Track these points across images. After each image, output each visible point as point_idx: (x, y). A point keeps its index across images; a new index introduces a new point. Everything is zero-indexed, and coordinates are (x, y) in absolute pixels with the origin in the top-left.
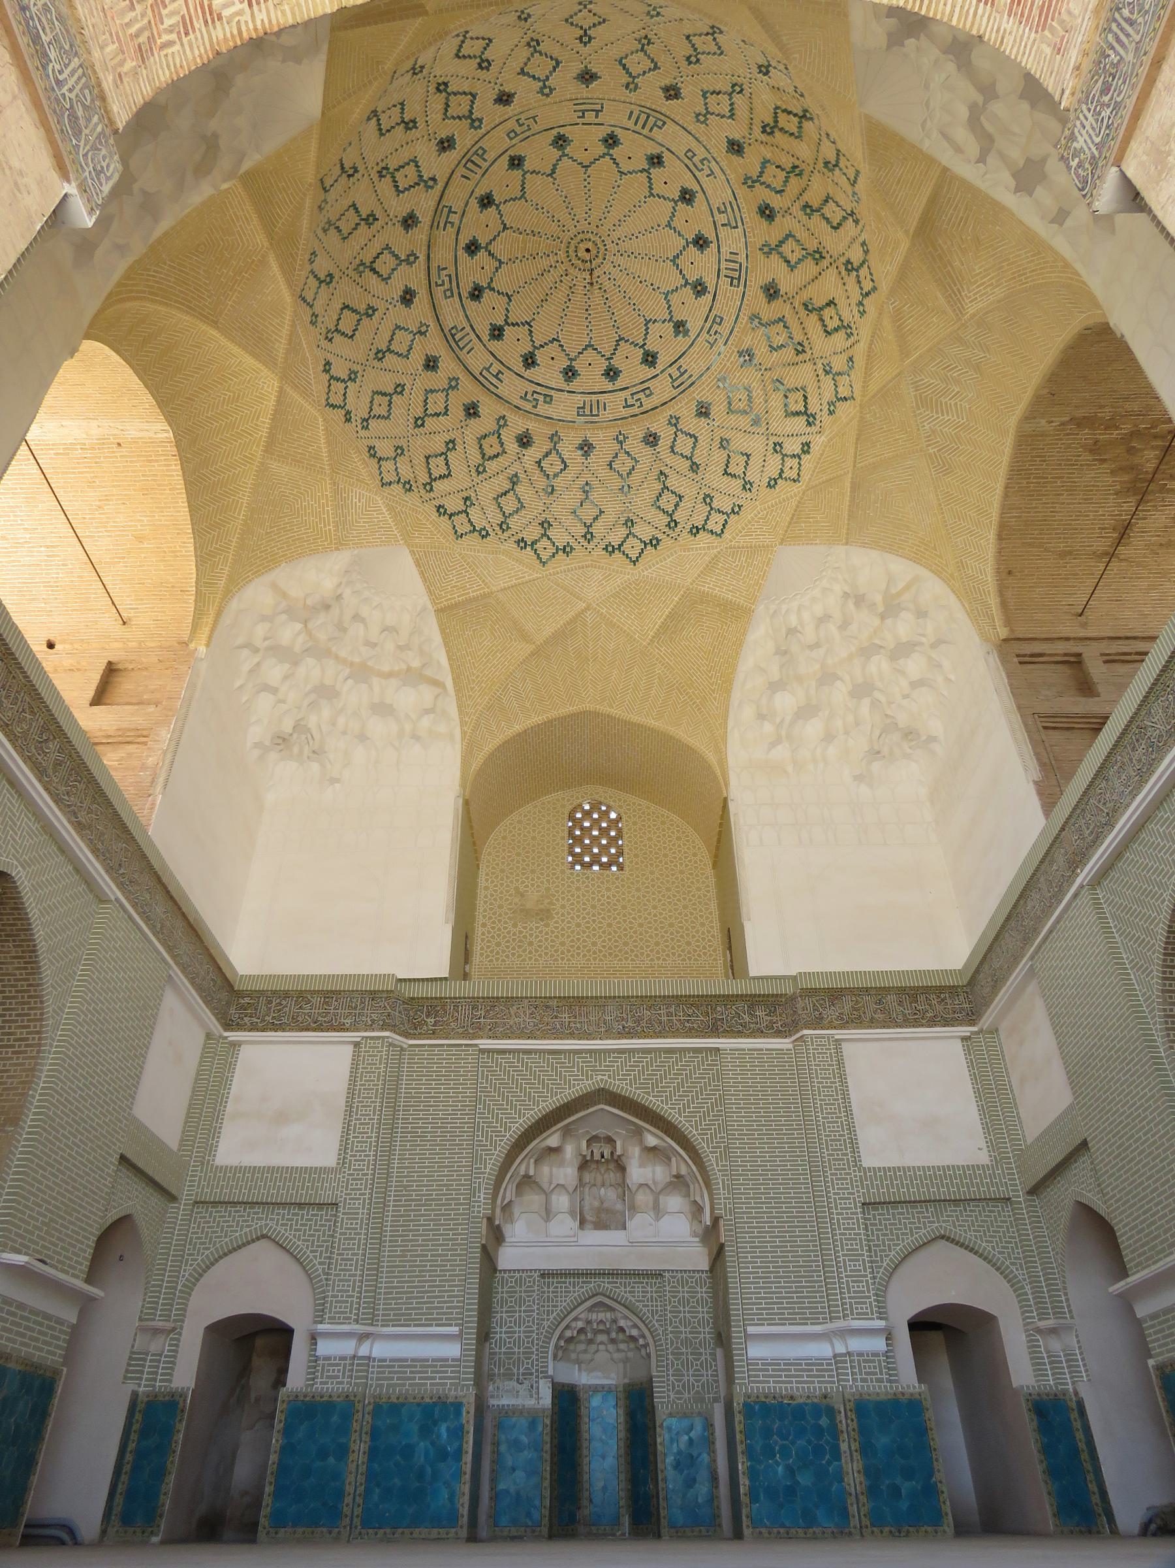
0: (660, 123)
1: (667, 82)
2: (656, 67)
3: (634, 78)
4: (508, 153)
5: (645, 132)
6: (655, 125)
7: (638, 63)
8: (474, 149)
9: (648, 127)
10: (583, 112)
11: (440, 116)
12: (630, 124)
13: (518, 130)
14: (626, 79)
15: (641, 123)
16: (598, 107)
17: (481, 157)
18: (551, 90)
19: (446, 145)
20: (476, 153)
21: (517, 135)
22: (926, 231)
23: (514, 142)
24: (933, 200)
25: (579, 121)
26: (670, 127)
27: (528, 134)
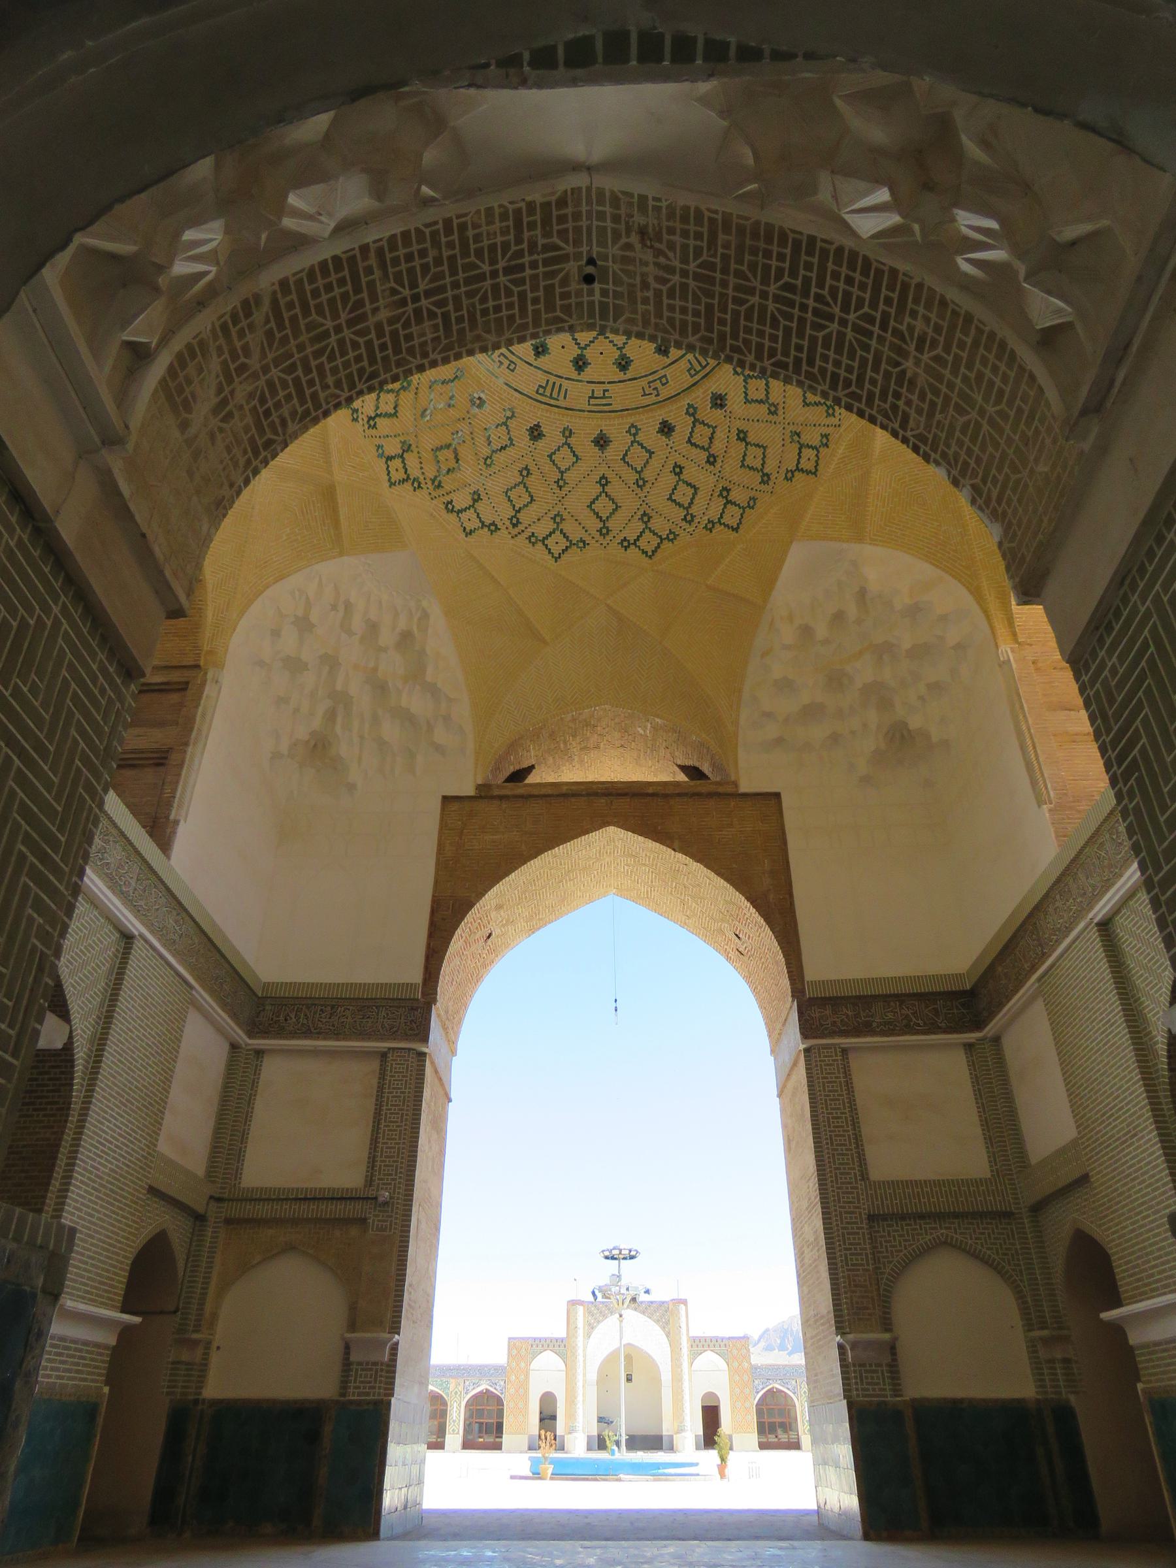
0: (541, 391)
1: (541, 444)
2: (550, 456)
3: (566, 443)
4: (669, 361)
5: (552, 379)
6: (544, 388)
7: (564, 458)
8: (697, 378)
9: (550, 384)
10: (604, 397)
11: (718, 430)
12: (566, 384)
13: (658, 384)
14: (572, 441)
15: (557, 386)
16: (593, 401)
17: (692, 367)
18: (629, 431)
19: (719, 401)
20: (697, 373)
21: (660, 379)
22: (329, 495)
23: (662, 373)
24: (336, 523)
25: (607, 386)
26: (531, 390)
27: (651, 378)
